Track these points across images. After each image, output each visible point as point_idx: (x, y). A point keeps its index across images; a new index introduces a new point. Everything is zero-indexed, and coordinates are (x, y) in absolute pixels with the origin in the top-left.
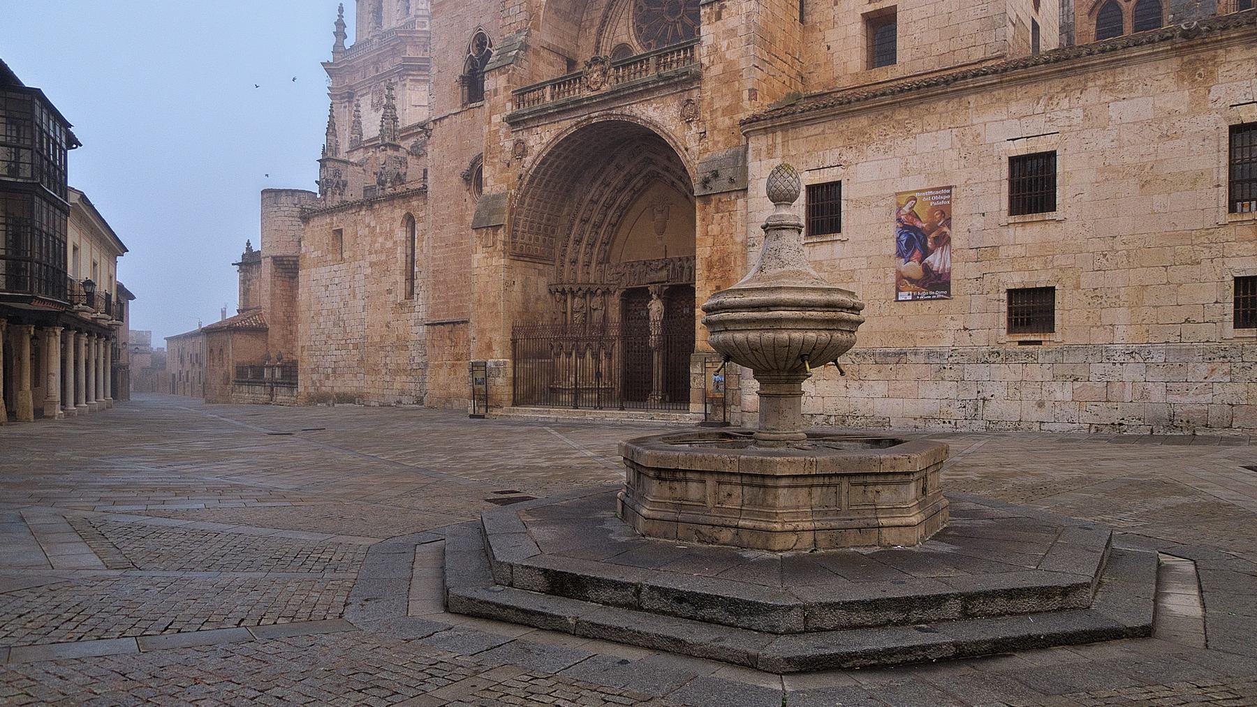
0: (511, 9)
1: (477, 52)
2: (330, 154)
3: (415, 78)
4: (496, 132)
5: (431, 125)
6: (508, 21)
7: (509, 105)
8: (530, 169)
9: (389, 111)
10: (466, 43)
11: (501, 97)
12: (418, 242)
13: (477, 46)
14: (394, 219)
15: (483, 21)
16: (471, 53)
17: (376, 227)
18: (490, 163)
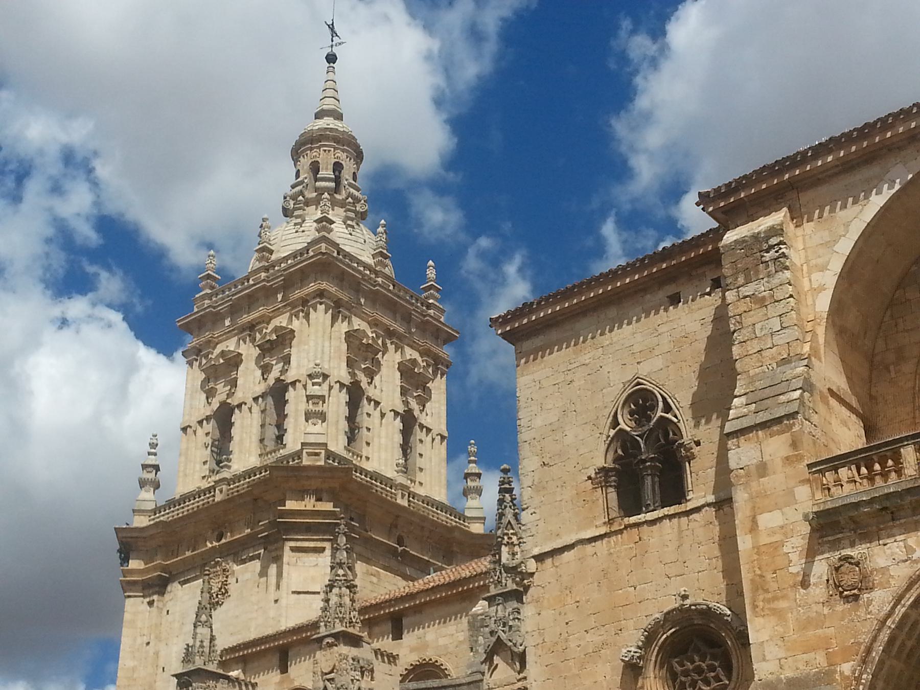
0: (758, 326)
1: (633, 424)
2: (199, 663)
3: (299, 544)
4: (776, 546)
5: (532, 566)
6: (753, 347)
7: (803, 492)
8: (890, 614)
9: (341, 572)
10: (607, 411)
11: (776, 481)
13: (631, 413)
15: (644, 370)
16: (623, 426)
18: (767, 612)
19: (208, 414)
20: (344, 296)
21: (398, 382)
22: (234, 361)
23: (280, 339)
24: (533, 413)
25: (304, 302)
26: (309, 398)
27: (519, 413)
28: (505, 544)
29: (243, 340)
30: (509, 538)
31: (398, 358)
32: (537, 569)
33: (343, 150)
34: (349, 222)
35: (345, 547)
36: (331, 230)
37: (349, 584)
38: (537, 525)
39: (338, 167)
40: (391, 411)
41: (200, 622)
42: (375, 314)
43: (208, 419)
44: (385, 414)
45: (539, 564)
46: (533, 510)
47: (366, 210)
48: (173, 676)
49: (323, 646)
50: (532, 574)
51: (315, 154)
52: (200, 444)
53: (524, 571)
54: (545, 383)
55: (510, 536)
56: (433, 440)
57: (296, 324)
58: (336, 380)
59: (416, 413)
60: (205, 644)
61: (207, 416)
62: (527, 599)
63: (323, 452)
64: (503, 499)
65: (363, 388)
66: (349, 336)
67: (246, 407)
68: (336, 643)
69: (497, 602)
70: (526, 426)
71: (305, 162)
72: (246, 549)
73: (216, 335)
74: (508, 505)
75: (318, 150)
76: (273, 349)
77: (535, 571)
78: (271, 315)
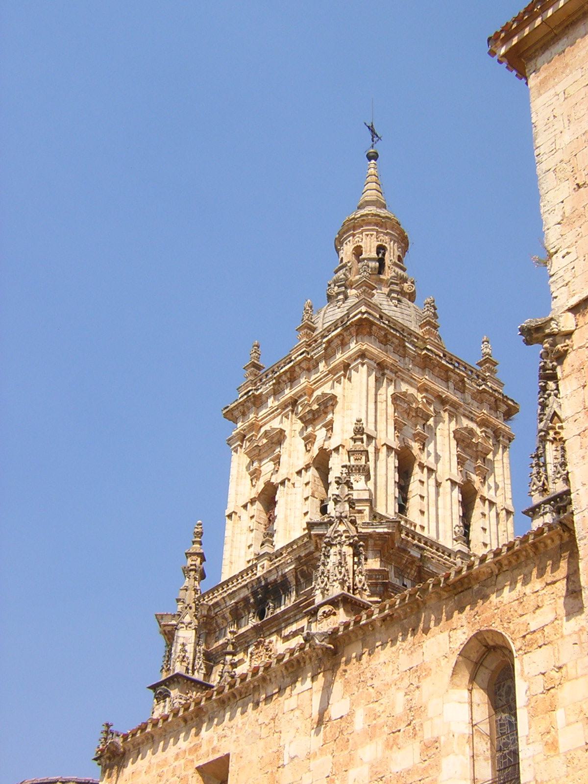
12: (532, 717)
14: (419, 672)
17: (351, 714)
19: (253, 497)
20: (390, 358)
21: (454, 451)
22: (278, 438)
23: (322, 408)
24: (558, 131)
25: (346, 367)
26: (350, 453)
27: (537, 141)
28: (550, 441)
29: (286, 417)
30: (556, 433)
31: (453, 426)
32: (577, 325)
33: (387, 234)
34: (393, 295)
35: (346, 499)
36: (373, 295)
37: (351, 541)
38: (574, 268)
39: (381, 249)
40: (447, 480)
41: (182, 623)
42: (424, 379)
43: (252, 502)
44: (441, 483)
45: (581, 319)
46: (564, 252)
47: (415, 291)
48: (149, 688)
49: (318, 619)
50: (569, 335)
51: (357, 240)
52: (245, 529)
53: (556, 330)
54: (571, 91)
55: (557, 430)
56: (498, 515)
57: (338, 390)
58: (383, 443)
59: (477, 485)
60: (187, 648)
61: (251, 499)
62: (563, 371)
63: (367, 509)
64: (545, 386)
65: (415, 454)
66: (395, 398)
67: (290, 483)
68: (334, 611)
69: (542, 512)
70: (547, 152)
71: (347, 250)
72: (289, 624)
73: (259, 419)
74: (552, 393)
75: (361, 236)
76: (317, 419)
77: (573, 329)
78: (313, 387)
